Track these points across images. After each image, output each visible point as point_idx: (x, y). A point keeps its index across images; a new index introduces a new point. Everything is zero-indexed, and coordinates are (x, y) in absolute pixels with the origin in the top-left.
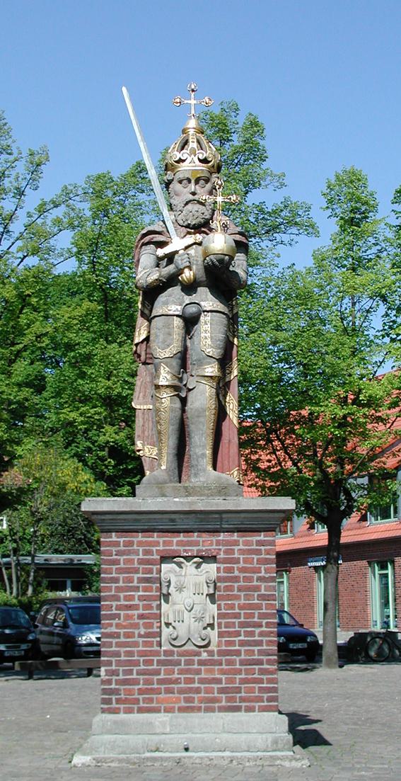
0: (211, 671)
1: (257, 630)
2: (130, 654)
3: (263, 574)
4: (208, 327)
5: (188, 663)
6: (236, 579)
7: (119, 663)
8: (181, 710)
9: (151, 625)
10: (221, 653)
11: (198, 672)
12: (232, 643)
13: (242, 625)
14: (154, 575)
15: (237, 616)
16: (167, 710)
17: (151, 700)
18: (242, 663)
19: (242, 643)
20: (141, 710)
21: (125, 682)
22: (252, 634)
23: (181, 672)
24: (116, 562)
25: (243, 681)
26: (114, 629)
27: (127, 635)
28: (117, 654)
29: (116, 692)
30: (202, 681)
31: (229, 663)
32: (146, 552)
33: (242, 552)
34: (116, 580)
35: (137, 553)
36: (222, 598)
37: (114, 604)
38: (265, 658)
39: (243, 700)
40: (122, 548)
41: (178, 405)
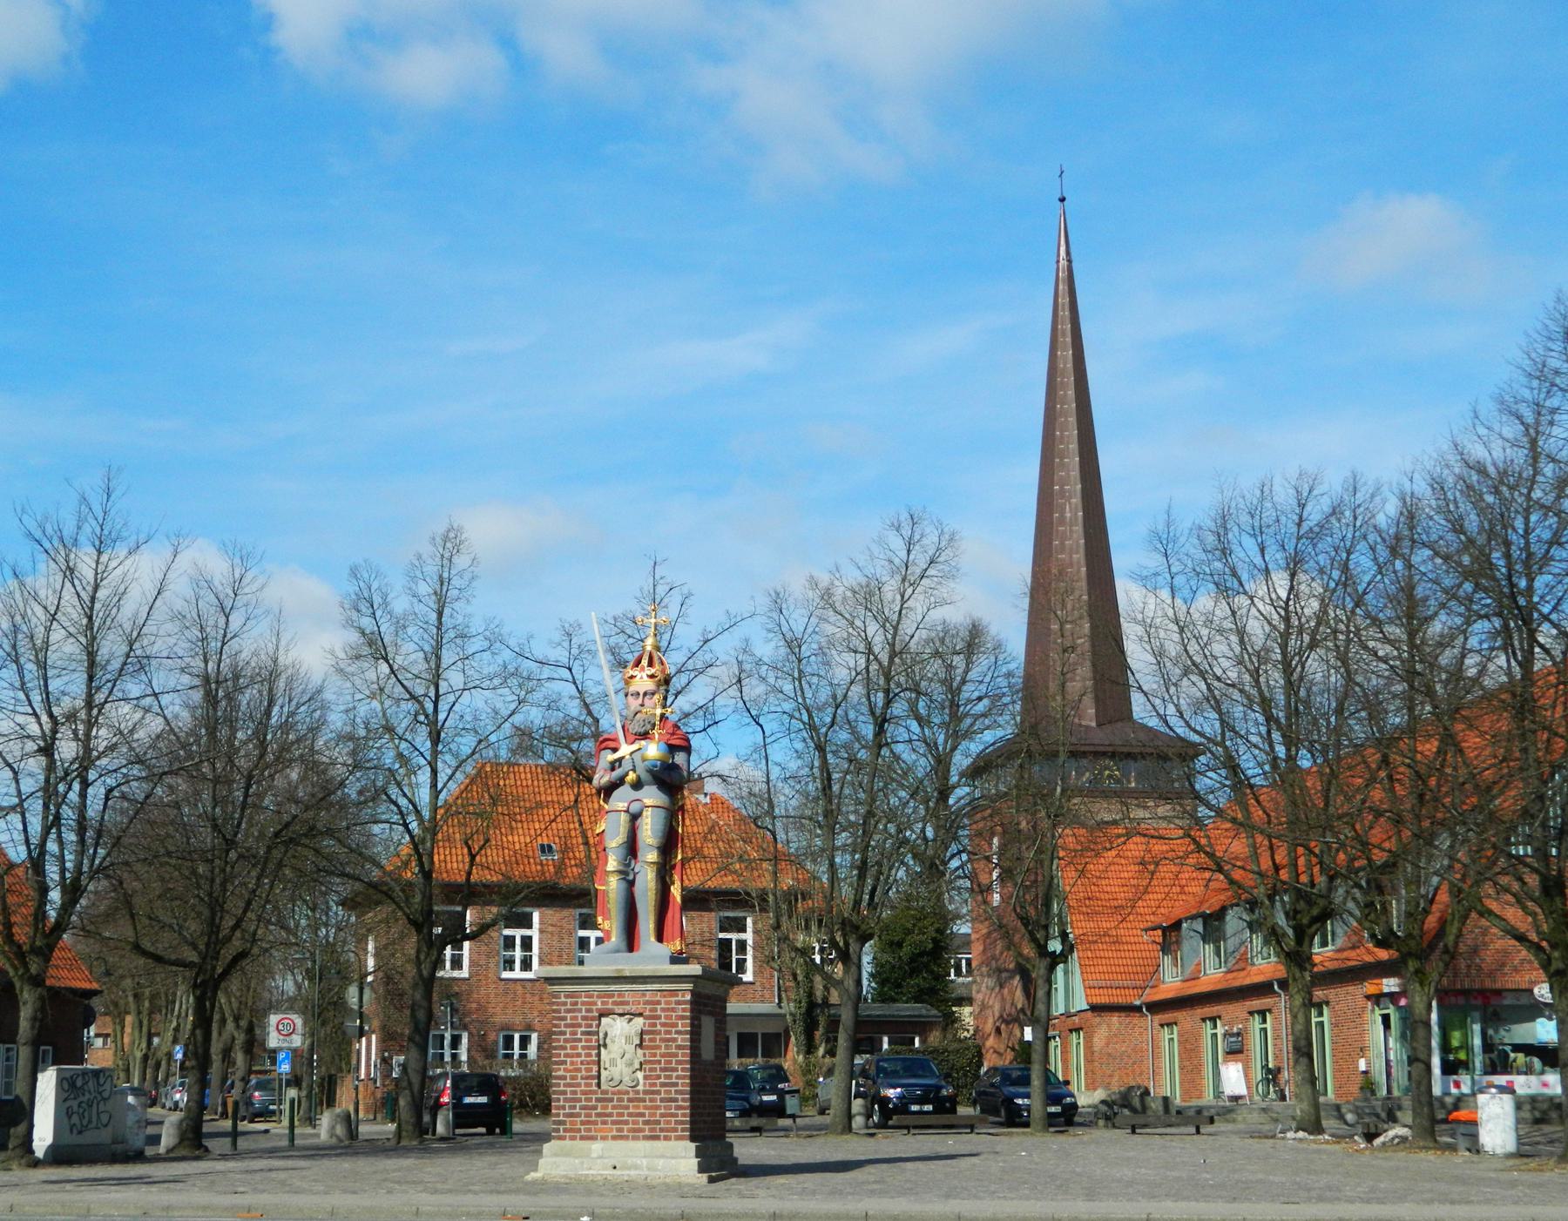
0: (638, 1107)
1: (675, 1074)
2: (574, 1093)
3: (680, 1028)
4: (649, 820)
5: (620, 1100)
6: (659, 1033)
7: (566, 1100)
8: (614, 1138)
9: (591, 1070)
10: (645, 1092)
11: (627, 1108)
12: (655, 1085)
13: (661, 1070)
14: (594, 1029)
15: (659, 1062)
16: (604, 1138)
17: (590, 1130)
18: (662, 1100)
19: (663, 1085)
20: (582, 1138)
21: (571, 1115)
22: (669, 1077)
23: (614, 1107)
24: (564, 1019)
25: (662, 1115)
26: (561, 1073)
27: (573, 1078)
28: (564, 1093)
29: (564, 1123)
30: (630, 1115)
31: (651, 1100)
32: (588, 1011)
33: (663, 1010)
34: (564, 1033)
35: (580, 1011)
36: (648, 1048)
37: (562, 1052)
38: (680, 1097)
39: (662, 1130)
40: (569, 1007)
41: (623, 885)
